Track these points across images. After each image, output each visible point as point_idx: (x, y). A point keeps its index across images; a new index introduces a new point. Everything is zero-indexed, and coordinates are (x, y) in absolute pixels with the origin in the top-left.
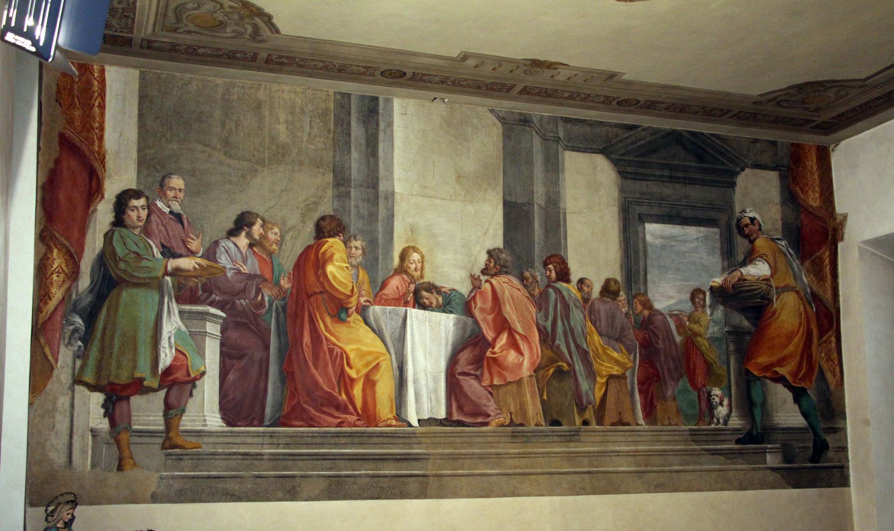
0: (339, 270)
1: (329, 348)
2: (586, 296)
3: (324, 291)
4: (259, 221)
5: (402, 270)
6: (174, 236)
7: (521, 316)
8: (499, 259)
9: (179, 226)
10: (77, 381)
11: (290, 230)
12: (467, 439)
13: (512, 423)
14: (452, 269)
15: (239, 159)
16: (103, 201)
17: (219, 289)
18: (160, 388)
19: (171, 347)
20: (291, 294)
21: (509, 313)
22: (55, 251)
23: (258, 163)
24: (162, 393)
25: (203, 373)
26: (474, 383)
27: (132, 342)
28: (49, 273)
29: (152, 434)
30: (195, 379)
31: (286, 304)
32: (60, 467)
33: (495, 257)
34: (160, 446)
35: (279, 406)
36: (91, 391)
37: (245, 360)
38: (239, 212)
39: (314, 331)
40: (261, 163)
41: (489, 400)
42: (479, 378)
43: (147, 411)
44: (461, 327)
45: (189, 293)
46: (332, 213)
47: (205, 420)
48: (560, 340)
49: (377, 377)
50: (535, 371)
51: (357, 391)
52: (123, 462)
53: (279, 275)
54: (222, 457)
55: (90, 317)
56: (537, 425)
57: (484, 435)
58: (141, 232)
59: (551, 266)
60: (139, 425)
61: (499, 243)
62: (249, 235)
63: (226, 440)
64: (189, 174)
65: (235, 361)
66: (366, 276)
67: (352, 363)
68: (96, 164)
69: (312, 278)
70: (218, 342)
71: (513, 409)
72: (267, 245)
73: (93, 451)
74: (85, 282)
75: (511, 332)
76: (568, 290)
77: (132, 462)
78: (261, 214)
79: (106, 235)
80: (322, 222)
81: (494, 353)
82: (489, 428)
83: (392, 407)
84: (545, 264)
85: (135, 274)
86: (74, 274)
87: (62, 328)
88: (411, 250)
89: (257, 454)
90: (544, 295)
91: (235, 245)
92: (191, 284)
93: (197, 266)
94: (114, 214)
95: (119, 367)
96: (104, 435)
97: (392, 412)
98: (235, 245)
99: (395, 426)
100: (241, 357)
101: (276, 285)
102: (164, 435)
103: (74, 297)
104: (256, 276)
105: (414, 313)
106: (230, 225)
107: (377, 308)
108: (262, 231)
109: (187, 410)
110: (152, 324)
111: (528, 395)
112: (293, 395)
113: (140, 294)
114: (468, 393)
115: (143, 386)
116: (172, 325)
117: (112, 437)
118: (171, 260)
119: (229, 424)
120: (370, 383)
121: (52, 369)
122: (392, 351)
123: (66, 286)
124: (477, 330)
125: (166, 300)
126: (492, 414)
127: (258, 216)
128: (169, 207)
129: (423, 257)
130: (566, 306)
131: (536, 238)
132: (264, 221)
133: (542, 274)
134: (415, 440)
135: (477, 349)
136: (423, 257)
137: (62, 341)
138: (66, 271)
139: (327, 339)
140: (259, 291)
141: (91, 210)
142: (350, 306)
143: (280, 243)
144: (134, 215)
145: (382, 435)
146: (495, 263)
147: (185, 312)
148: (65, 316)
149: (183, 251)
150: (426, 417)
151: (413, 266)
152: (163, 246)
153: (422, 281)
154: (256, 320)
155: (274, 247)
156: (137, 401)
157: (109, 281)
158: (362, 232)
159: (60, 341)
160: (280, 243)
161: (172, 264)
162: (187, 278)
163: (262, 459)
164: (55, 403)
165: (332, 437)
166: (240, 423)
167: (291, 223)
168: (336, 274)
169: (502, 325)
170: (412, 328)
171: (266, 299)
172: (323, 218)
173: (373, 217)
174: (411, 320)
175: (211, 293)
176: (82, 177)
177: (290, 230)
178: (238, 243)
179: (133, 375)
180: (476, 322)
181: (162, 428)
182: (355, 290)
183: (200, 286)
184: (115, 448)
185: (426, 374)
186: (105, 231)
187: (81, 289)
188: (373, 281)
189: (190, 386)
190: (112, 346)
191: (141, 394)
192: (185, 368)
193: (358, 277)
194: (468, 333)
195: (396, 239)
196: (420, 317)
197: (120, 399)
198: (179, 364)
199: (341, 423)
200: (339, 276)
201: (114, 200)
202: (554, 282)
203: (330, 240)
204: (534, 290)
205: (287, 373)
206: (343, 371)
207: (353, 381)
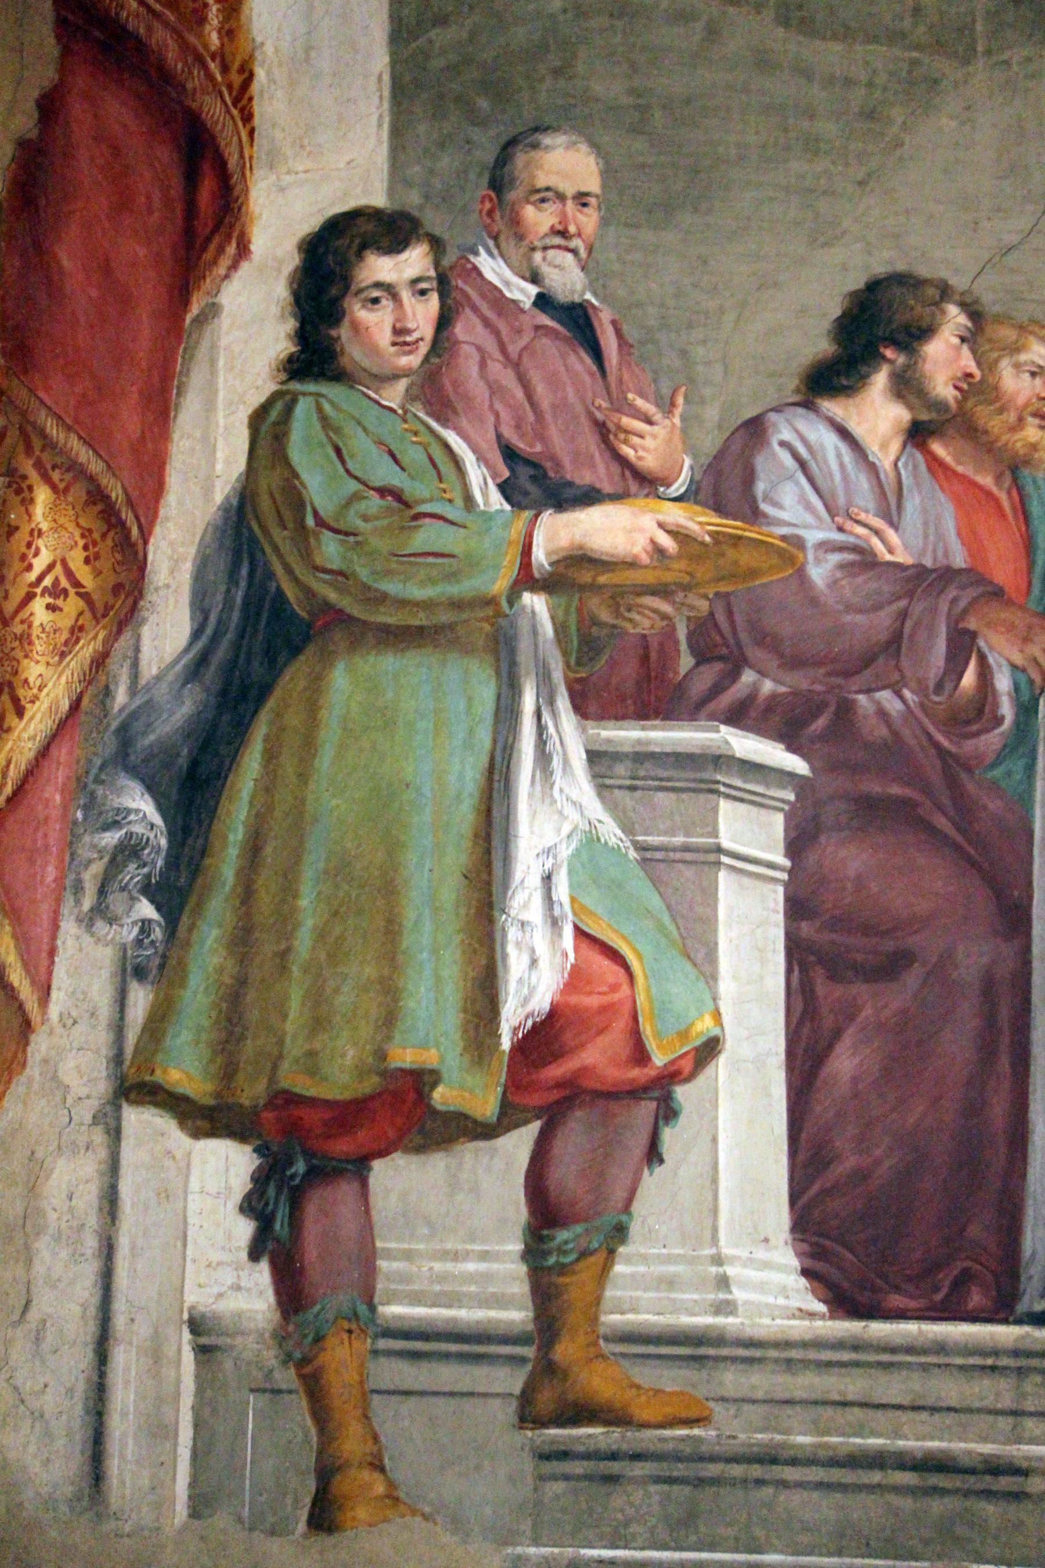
4: (955, 318)
6: (561, 407)
9: (581, 362)
10: (135, 1085)
15: (846, 34)
16: (245, 267)
18: (508, 1119)
19: (555, 923)
22: (42, 496)
23: (939, 46)
24: (518, 1145)
25: (710, 1049)
27: (374, 900)
28: (17, 595)
29: (471, 1344)
30: (672, 1076)
32: (49, 1503)
34: (513, 1405)
36: (197, 1134)
37: (912, 978)
38: (856, 281)
40: (955, 42)
43: (447, 1235)
45: (630, 669)
47: (724, 1282)
52: (341, 1485)
54: (816, 1474)
55: (193, 788)
58: (410, 396)
60: (416, 1299)
62: (907, 386)
63: (833, 1385)
64: (621, 126)
65: (860, 990)
68: (214, 110)
72: (995, 424)
73: (198, 1426)
74: (167, 631)
77: (380, 1489)
78: (959, 282)
79: (258, 418)
85: (392, 587)
86: (121, 600)
87: (71, 843)
89: (994, 1468)
91: (843, 433)
92: (642, 623)
93: (666, 541)
94: (291, 325)
95: (318, 1022)
96: (248, 1347)
98: (843, 433)
100: (890, 967)
102: (529, 1351)
103: (121, 696)
104: (946, 575)
106: (817, 344)
108: (967, 361)
109: (635, 1229)
110: (465, 815)
113: (408, 679)
115: (435, 1113)
116: (557, 818)
117: (287, 1359)
118: (548, 518)
119: (844, 1302)
121: (26, 1027)
123: (86, 650)
125: (529, 702)
127: (945, 291)
128: (535, 278)
132: (975, 314)
137: (67, 908)
138: (84, 575)
140: (962, 645)
141: (195, 310)
144: (376, 322)
147: (616, 757)
148: (86, 791)
149: (599, 473)
152: (510, 454)
154: (953, 784)
156: (400, 1181)
157: (270, 628)
159: (59, 901)
161: (555, 533)
162: (619, 598)
163: (1018, 1496)
164: (32, 1190)
166: (896, 1301)
171: (1003, 683)
175: (737, 664)
176: (155, 166)
179: (381, 1055)
181: (518, 1315)
183: (682, 633)
184: (298, 1411)
186: (258, 398)
187: (150, 668)
189: (647, 1108)
190: (286, 921)
191: (420, 1149)
192: (620, 1025)
197: (323, 1172)
198: (593, 1001)
201: (293, 261)
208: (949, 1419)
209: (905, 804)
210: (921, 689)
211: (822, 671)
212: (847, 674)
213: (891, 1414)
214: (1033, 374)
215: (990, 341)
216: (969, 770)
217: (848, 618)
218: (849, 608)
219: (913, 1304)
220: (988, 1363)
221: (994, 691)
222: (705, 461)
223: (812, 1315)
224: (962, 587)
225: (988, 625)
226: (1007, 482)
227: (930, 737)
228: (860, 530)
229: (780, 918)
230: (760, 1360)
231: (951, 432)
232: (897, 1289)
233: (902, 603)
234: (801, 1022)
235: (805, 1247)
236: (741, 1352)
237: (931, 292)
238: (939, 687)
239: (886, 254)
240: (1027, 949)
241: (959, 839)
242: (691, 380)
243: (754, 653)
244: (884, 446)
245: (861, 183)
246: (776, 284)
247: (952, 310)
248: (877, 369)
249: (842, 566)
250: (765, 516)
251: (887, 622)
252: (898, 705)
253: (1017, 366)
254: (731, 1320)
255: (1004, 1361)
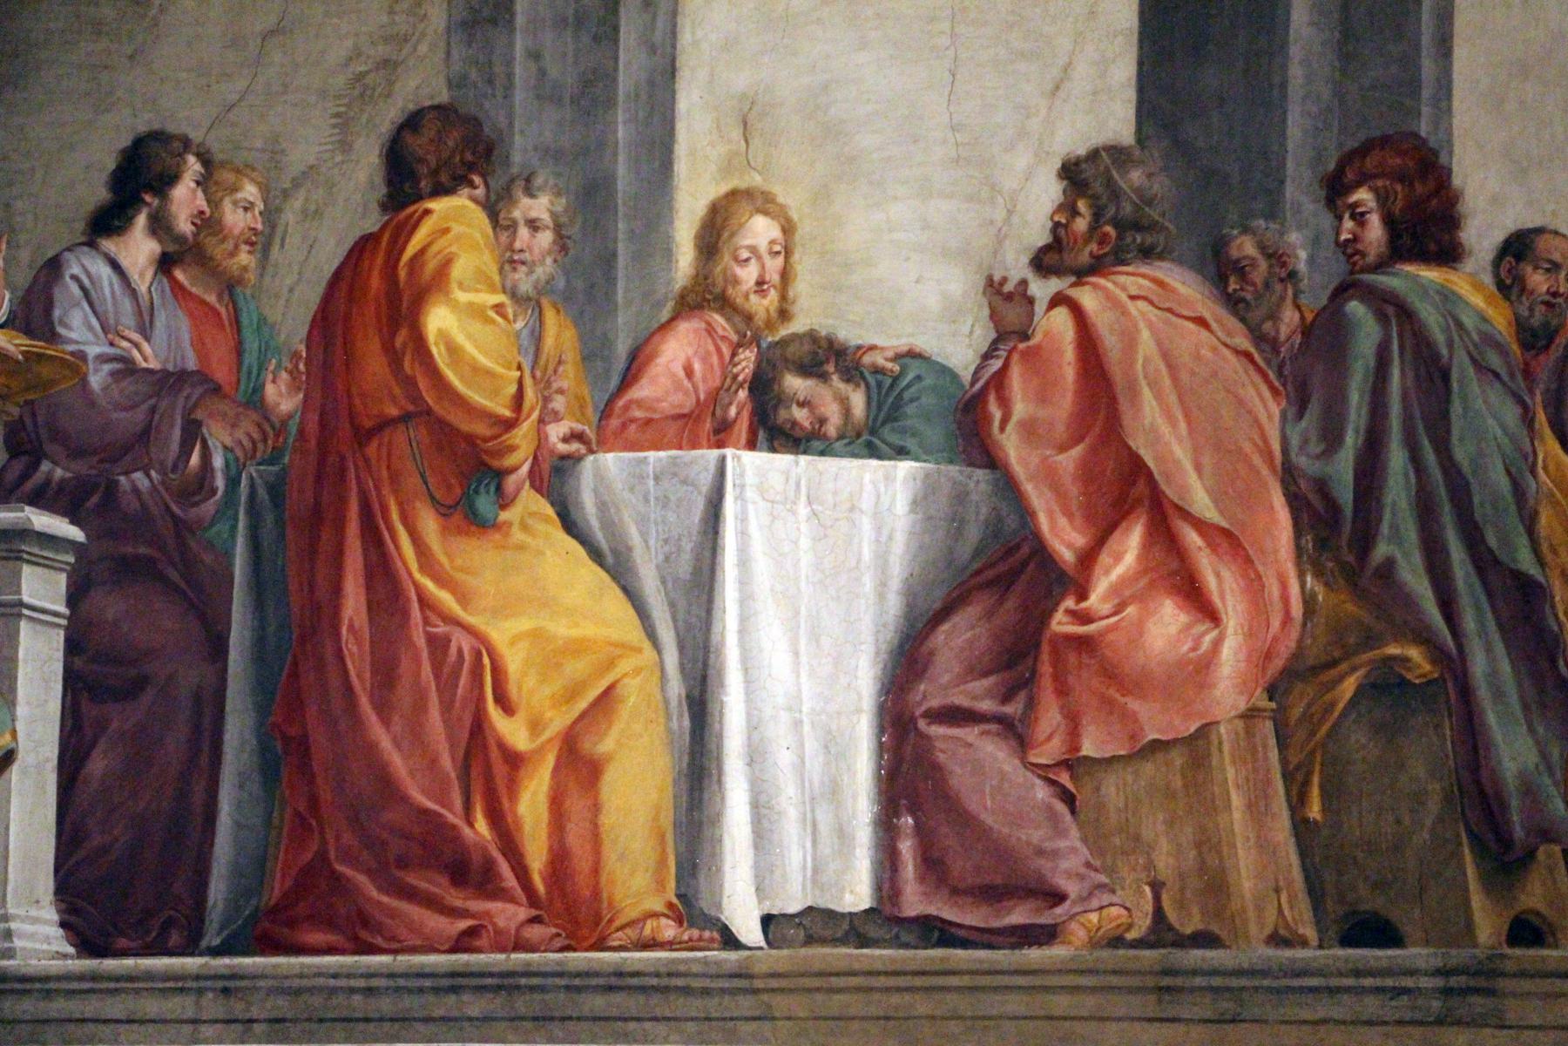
0: (468, 329)
1: (432, 639)
2: (1536, 321)
3: (418, 413)
4: (193, 165)
5: (705, 296)
7: (1213, 443)
8: (1115, 194)
11: (296, 184)
12: (963, 1004)
13: (1161, 933)
14: (904, 271)
17: (58, 436)
20: (301, 432)
21: (1155, 438)
26: (994, 752)
31: (282, 476)
33: (1098, 187)
35: (252, 871)
37: (147, 697)
38: (125, 141)
39: (381, 570)
41: (1060, 832)
42: (1017, 734)
44: (940, 515)
46: (444, 97)
48: (1396, 536)
49: (606, 745)
50: (1271, 692)
51: (531, 804)
53: (262, 367)
56: (1275, 940)
57: (1037, 981)
59: (1363, 195)
61: (1115, 120)
62: (160, 225)
66: (570, 334)
67: (513, 690)
69: (373, 364)
70: (59, 637)
71: (1164, 863)
72: (218, 251)
75: (1164, 518)
76: (1447, 297)
78: (196, 136)
80: (409, 138)
81: (1084, 618)
82: (1056, 952)
83: (662, 862)
84: (1335, 189)
88: (744, 206)
90: (1326, 334)
91: (115, 265)
97: (660, 884)
98: (115, 265)
99: (669, 945)
100: (137, 687)
101: (248, 405)
105: (755, 471)
106: (98, 193)
107: (612, 462)
108: (201, 202)
111: (1237, 800)
112: (303, 826)
114: (972, 804)
119: (88, 945)
120: (579, 766)
122: (667, 636)
124: (1012, 522)
126: (1072, 888)
127: (186, 143)
129: (788, 229)
130: (1433, 376)
131: (1296, 72)
132: (206, 160)
133: (1316, 241)
134: (746, 1005)
135: (1011, 604)
136: (788, 229)
139: (425, 602)
140: (192, 432)
142: (510, 461)
143: (263, 241)
145: (617, 982)
146: (1097, 216)
150: (793, 908)
151: (748, 275)
153: (784, 332)
155: (244, 257)
158: (554, 155)
160: (263, 241)
165: (436, 990)
166: (122, 942)
167: (299, 156)
168: (460, 339)
169: (1125, 488)
170: (743, 534)
171: (218, 462)
172: (412, 122)
173: (592, 93)
174: (740, 497)
175: (37, 458)
177: (296, 184)
178: (125, 263)
180: (1008, 486)
182: (530, 394)
185: (798, 724)
188: (593, 353)
193: (538, 338)
194: (973, 534)
195: (681, 167)
196: (776, 481)
199: (472, 932)
200: (469, 347)
202: (1380, 266)
203: (438, 205)
204: (1274, 316)
205: (286, 740)
206: (479, 725)
207: (515, 761)
208: (151, 1028)
209: (151, 561)
210: (163, 472)
211: (96, 459)
212: (114, 461)
213: (112, 1026)
214: (246, 209)
215: (216, 183)
216: (194, 533)
217: (115, 415)
218: (118, 407)
219: (133, 945)
220: (177, 984)
221: (212, 470)
222: (20, 293)
223: (65, 956)
224: (193, 386)
225: (211, 415)
226: (226, 297)
227: (168, 508)
228: (125, 344)
229: (60, 655)
230: (29, 991)
231: (188, 258)
232: (122, 934)
233: (152, 401)
234: (70, 736)
235: (63, 906)
236: (18, 986)
237: (176, 144)
238: (175, 468)
239: (146, 116)
240: (225, 670)
241: (183, 585)
242: (13, 230)
243: (48, 447)
244: (142, 275)
245: (131, 57)
246: (72, 148)
247: (191, 159)
248: (139, 211)
249: (112, 374)
250: (60, 336)
251: (141, 417)
252: (146, 482)
253: (235, 203)
254: (11, 962)
255: (190, 984)
